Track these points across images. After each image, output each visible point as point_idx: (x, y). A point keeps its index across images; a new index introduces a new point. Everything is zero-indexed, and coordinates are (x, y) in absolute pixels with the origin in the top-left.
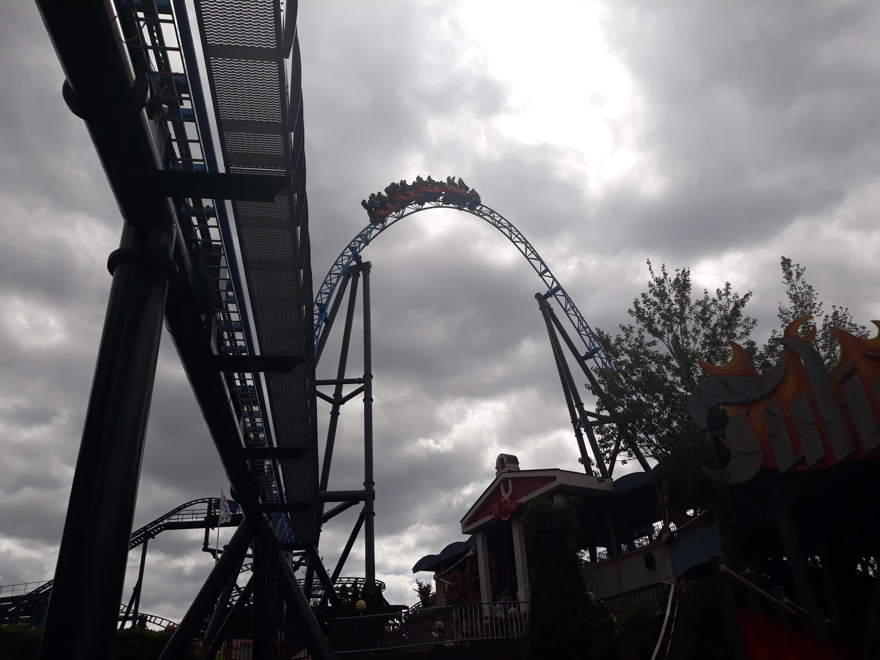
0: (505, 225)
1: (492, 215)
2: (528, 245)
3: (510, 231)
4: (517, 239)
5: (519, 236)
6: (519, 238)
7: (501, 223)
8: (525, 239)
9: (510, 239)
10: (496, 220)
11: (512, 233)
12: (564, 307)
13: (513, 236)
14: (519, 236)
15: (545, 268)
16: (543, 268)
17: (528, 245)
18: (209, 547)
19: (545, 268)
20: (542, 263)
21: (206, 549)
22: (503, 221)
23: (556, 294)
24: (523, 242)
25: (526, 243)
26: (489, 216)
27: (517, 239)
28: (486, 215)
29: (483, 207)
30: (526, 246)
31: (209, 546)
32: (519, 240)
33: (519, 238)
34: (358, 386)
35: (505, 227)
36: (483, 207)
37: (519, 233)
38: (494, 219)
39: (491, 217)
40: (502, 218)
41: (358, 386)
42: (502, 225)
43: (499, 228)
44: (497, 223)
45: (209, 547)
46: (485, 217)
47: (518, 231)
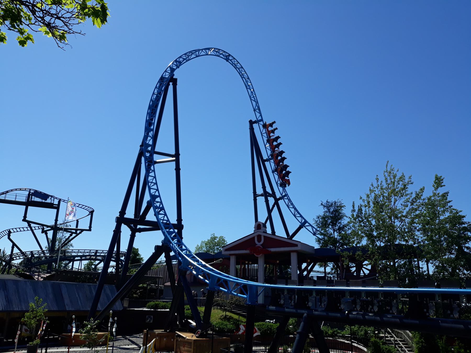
0: (245, 77)
1: (247, 80)
2: (257, 104)
3: (252, 92)
4: (253, 99)
5: (255, 98)
6: (254, 99)
7: (249, 86)
8: (257, 100)
9: (250, 97)
10: (247, 84)
11: (252, 94)
12: (287, 204)
13: (252, 96)
14: (255, 98)
15: (261, 118)
16: (260, 118)
17: (257, 104)
18: (27, 219)
19: (261, 118)
20: (261, 115)
21: (24, 220)
22: (251, 86)
23: (270, 161)
24: (255, 102)
25: (257, 102)
26: (245, 79)
27: (253, 99)
28: (238, 68)
29: (238, 64)
30: (256, 104)
31: (27, 218)
32: (254, 100)
33: (254, 99)
34: (151, 186)
35: (250, 90)
36: (238, 64)
37: (256, 96)
38: (247, 83)
39: (246, 81)
40: (246, 73)
41: (151, 186)
42: (250, 88)
43: (247, 88)
44: (252, 96)
45: (27, 219)
46: (244, 79)
47: (255, 95)
